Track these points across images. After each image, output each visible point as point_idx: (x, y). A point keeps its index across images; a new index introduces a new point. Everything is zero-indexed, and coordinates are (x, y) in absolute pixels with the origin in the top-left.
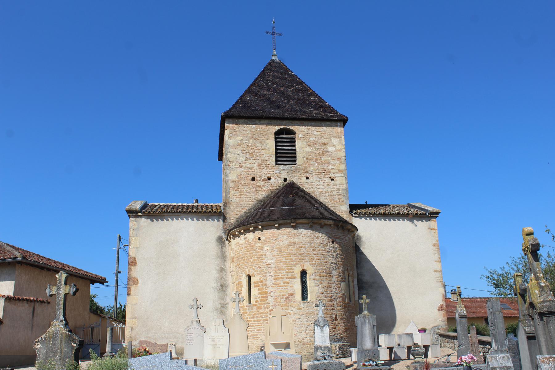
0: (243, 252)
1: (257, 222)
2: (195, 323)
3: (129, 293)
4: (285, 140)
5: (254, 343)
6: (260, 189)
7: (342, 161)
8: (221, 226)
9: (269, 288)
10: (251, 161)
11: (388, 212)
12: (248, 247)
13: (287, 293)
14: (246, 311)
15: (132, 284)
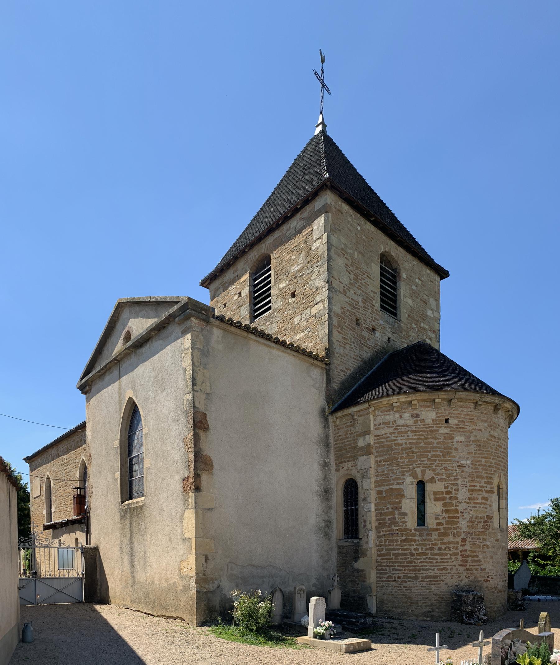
5: (430, 589)
13: (484, 515)
14: (413, 538)
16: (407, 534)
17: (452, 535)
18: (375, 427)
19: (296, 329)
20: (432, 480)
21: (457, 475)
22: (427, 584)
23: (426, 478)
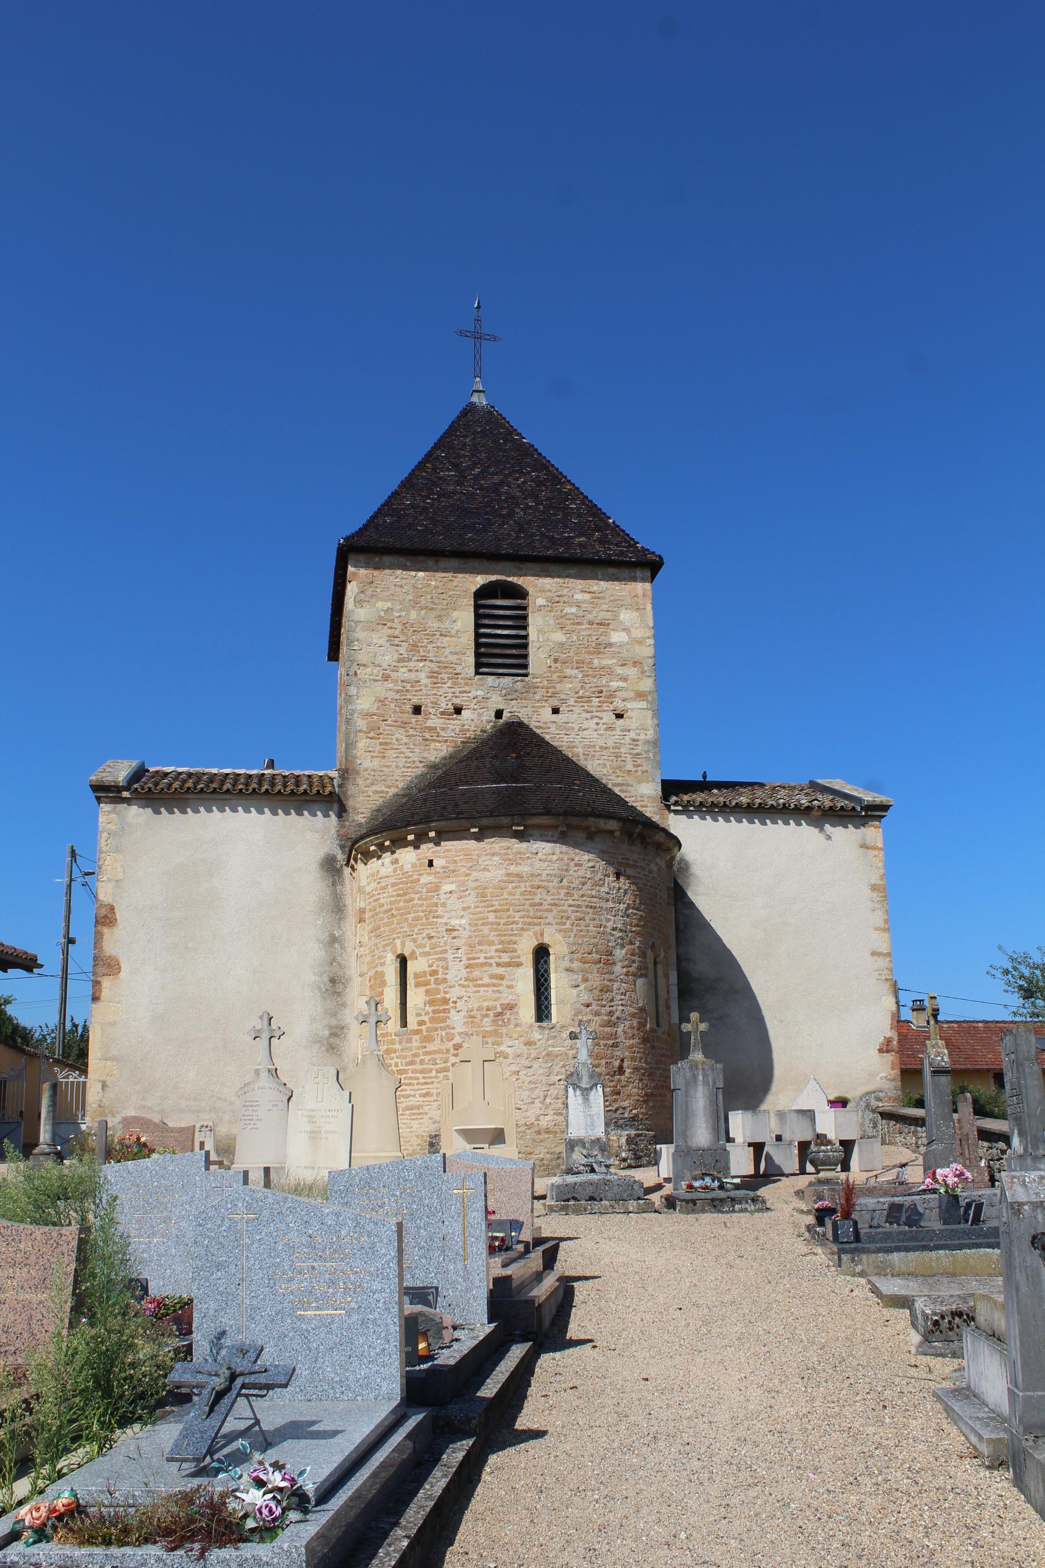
0: (388, 897)
1: (426, 820)
2: (264, 1075)
3: (97, 994)
4: (502, 612)
6: (435, 738)
7: (645, 668)
8: (333, 831)
10: (411, 664)
11: (759, 801)
12: (400, 883)
15: (106, 972)
21: (445, 943)
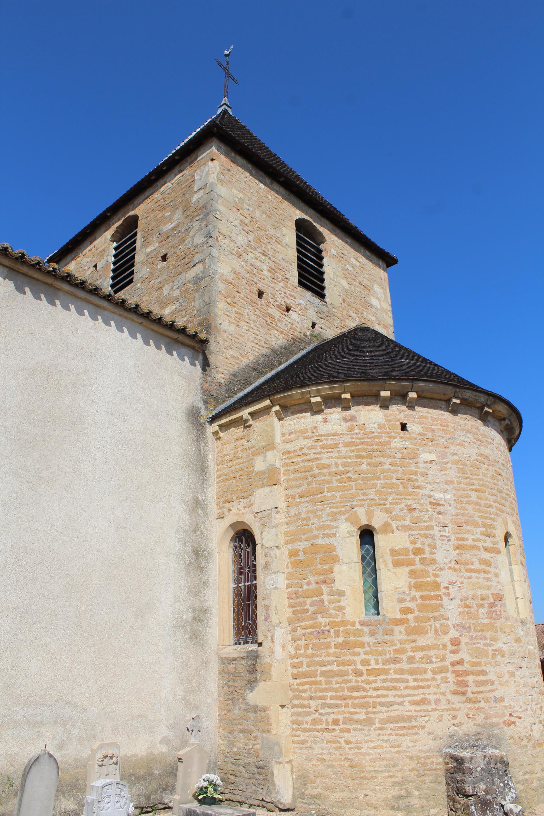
0: (338, 458)
5: (399, 746)
6: (273, 325)
7: (390, 332)
9: (444, 572)
13: (488, 593)
14: (359, 639)
16: (347, 633)
17: (433, 632)
18: (283, 438)
19: (164, 304)
20: (387, 528)
22: (391, 734)
23: (376, 524)
